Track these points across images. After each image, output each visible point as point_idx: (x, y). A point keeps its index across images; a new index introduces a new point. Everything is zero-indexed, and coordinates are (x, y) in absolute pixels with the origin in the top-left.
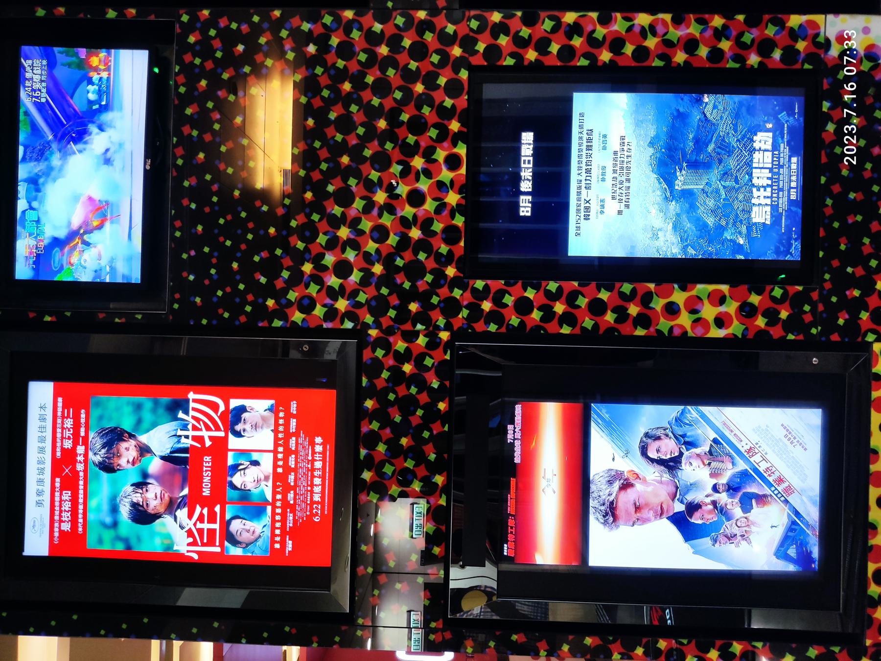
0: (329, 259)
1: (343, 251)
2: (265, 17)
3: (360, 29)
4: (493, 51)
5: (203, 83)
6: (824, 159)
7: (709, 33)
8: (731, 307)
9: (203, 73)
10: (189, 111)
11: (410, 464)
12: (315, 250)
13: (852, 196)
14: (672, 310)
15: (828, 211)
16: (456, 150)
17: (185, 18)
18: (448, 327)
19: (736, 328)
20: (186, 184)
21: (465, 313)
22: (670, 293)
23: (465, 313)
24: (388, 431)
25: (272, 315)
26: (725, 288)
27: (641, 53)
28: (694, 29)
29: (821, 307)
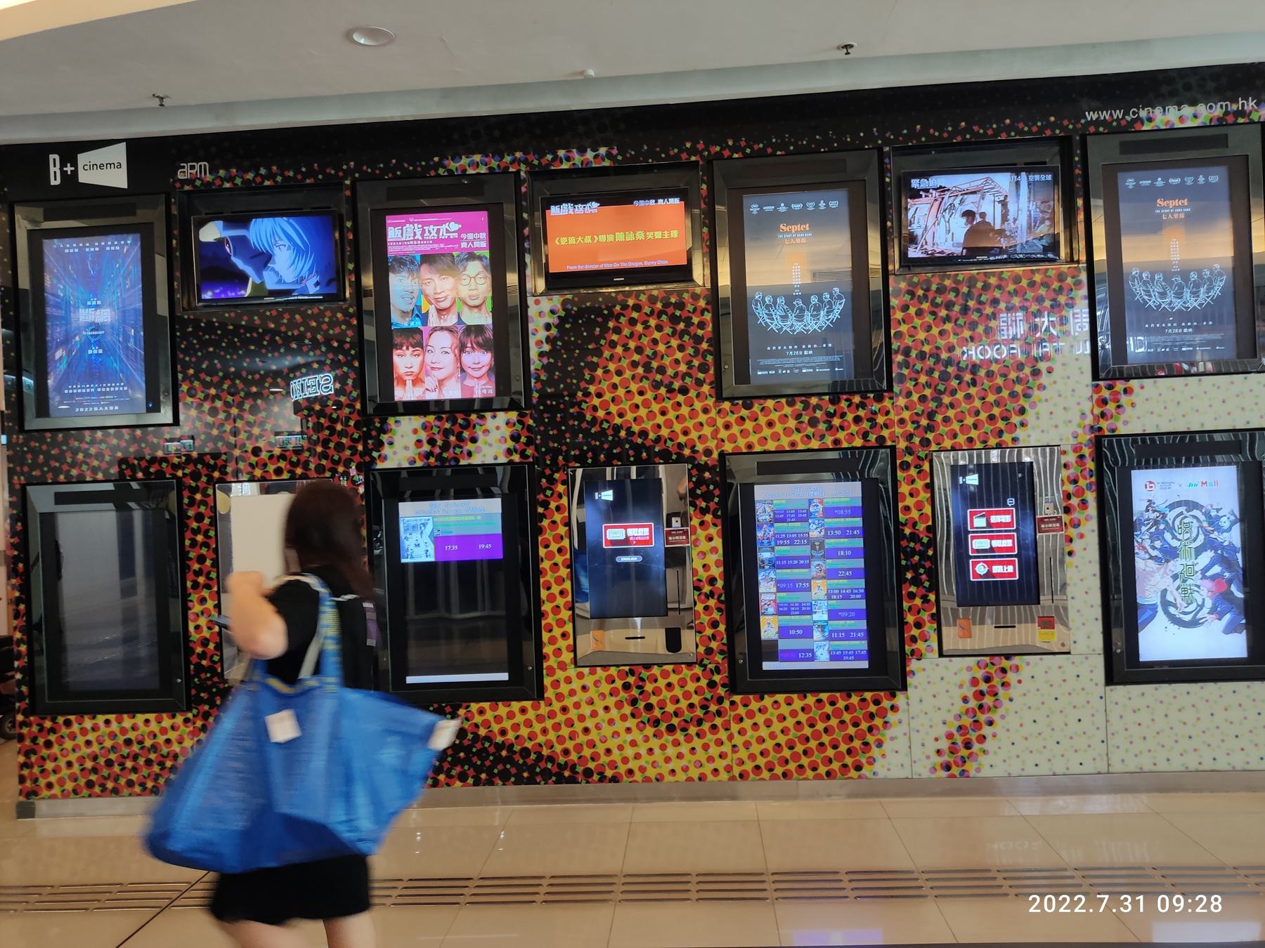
0: (219, 404)
1: (224, 411)
2: (354, 357)
3: (350, 413)
5: (314, 324)
8: (206, 633)
9: (320, 323)
10: (297, 317)
12: (223, 395)
14: (203, 600)
16: (285, 472)
18: (185, 475)
19: (195, 636)
20: (256, 318)
21: (193, 484)
23: (193, 484)
24: (124, 444)
29: (209, 683)
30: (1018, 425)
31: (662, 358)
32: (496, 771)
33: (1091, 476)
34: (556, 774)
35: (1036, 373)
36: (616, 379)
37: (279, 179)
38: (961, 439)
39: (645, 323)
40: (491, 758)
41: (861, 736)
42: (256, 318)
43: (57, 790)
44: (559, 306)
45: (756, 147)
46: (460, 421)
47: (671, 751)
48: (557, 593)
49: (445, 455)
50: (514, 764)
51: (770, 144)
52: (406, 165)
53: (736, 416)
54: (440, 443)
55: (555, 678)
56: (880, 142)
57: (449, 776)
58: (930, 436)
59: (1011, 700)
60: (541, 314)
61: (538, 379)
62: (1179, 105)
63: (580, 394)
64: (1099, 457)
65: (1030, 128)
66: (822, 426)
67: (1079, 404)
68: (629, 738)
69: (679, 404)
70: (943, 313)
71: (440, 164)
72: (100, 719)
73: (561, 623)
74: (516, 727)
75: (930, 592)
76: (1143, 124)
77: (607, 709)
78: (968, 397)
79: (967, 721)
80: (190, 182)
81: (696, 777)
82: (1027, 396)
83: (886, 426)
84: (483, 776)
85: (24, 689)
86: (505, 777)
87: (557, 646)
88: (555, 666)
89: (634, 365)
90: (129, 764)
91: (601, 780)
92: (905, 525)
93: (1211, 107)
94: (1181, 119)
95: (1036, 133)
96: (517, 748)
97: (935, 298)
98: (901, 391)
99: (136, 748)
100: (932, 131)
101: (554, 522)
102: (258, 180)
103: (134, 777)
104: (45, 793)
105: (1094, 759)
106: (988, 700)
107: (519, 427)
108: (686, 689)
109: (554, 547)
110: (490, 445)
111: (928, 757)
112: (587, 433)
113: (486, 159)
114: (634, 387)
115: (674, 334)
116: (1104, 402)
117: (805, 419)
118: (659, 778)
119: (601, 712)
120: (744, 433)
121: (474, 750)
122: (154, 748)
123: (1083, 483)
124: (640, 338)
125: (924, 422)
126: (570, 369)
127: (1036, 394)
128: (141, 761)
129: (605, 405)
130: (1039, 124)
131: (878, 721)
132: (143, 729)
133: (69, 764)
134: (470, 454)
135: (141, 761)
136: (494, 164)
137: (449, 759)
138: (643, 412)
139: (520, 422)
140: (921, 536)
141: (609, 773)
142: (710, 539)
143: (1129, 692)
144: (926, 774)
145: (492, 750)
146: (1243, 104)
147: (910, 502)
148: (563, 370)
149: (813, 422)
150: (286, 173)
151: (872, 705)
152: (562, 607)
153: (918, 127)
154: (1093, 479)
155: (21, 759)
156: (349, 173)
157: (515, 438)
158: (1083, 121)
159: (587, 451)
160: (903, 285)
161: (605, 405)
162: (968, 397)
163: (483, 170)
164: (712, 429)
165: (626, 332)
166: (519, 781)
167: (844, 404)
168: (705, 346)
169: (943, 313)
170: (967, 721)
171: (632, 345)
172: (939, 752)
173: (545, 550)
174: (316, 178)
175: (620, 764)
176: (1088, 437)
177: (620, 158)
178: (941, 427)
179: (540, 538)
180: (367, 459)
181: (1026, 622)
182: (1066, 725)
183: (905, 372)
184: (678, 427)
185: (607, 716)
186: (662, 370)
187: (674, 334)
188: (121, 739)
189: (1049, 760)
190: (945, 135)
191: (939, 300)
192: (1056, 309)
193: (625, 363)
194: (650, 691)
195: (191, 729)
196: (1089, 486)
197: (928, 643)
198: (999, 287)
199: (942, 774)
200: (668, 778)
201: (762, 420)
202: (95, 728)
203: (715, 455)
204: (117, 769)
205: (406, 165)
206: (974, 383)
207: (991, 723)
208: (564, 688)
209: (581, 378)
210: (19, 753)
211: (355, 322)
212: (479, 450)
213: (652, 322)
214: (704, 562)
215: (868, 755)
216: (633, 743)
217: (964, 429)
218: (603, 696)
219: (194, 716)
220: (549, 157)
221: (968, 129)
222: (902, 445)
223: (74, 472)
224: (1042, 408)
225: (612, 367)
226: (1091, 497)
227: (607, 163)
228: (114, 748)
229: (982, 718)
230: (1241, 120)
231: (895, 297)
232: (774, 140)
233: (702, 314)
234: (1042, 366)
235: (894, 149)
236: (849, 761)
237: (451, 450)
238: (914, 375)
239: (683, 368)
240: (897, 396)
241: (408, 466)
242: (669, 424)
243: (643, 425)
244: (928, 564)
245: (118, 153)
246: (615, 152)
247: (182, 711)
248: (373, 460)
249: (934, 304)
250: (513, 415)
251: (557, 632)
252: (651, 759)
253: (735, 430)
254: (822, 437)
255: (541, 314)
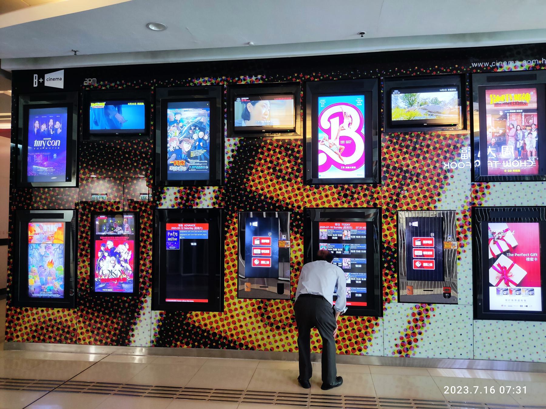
2: (151, 161)
4: (143, 217)
5: (136, 147)
6: (118, 297)
7: (147, 269)
8: (84, 275)
10: (129, 143)
11: (49, 200)
13: (110, 304)
14: (84, 261)
15: (106, 298)
17: (151, 141)
19: (80, 277)
22: (88, 261)
25: (82, 165)
26: (89, 274)
27: (143, 253)
28: (148, 266)
29: (84, 297)
30: (437, 200)
31: (281, 166)
32: (202, 342)
33: (470, 225)
34: (227, 345)
35: (446, 178)
36: (261, 174)
37: (125, 86)
38: (411, 206)
39: (274, 150)
40: (200, 336)
41: (361, 336)
42: (112, 143)
43: (20, 339)
44: (238, 142)
45: (325, 76)
46: (194, 190)
47: (278, 338)
48: (231, 266)
49: (187, 204)
50: (210, 339)
51: (331, 75)
52: (177, 81)
53: (312, 192)
54: (185, 199)
55: (229, 302)
56: (379, 75)
57: (181, 343)
58: (397, 204)
59: (430, 324)
60: (230, 145)
61: (228, 173)
62: (514, 61)
63: (245, 180)
64: (473, 217)
65: (446, 70)
66: (349, 198)
67: (465, 192)
68: (259, 331)
69: (287, 186)
70: (405, 150)
71: (191, 81)
72: (40, 309)
73: (232, 279)
74: (211, 323)
75: (395, 273)
76: (498, 69)
77: (250, 317)
78: (415, 187)
79: (409, 332)
80: (89, 86)
81: (288, 350)
82: (441, 188)
83: (378, 199)
84: (196, 344)
85: (10, 295)
86: (205, 345)
87: (230, 289)
88: (229, 297)
89: (269, 168)
90: (50, 329)
91: (246, 349)
92: (384, 243)
93: (529, 62)
94: (515, 67)
95: (449, 72)
96: (211, 332)
97: (401, 143)
98: (385, 183)
99: (53, 322)
100: (402, 70)
101: (231, 235)
102: (116, 86)
103: (52, 335)
104: (16, 339)
105: (467, 353)
106: (420, 323)
107: (218, 193)
108: (285, 310)
109: (231, 245)
110: (206, 200)
111: (391, 347)
112: (247, 196)
113: (210, 79)
114: (268, 178)
115: (286, 155)
116: (476, 192)
117: (342, 194)
118: (272, 349)
119: (248, 318)
120: (315, 199)
121: (193, 332)
122: (61, 323)
123: (466, 227)
124: (272, 157)
125: (395, 198)
126: (241, 169)
127: (446, 187)
128: (55, 328)
129: (255, 185)
130: (451, 68)
131: (370, 330)
132: (57, 315)
133: (26, 328)
134: (197, 204)
135: (55, 328)
136: (213, 81)
137: (182, 335)
138: (272, 189)
139: (219, 191)
140: (392, 248)
141: (250, 346)
142: (298, 245)
143: (484, 323)
144: (390, 355)
145: (200, 332)
146: (544, 61)
147: (387, 232)
148: (238, 169)
149: (346, 196)
150: (128, 84)
151: (347, 321)
152: (233, 272)
153: (396, 69)
154: (471, 226)
155: (7, 324)
156: (153, 84)
157: (217, 197)
158: (470, 67)
159: (247, 205)
160: (387, 137)
161: (255, 185)
162: (415, 187)
163: (209, 84)
164: (301, 197)
165: (266, 154)
166: (212, 347)
167: (359, 188)
168: (299, 161)
169: (405, 150)
170: (409, 332)
171: (268, 159)
172: (396, 345)
173: (227, 247)
174: (140, 86)
175: (255, 342)
176: (469, 207)
177: (266, 80)
178: (403, 200)
179: (225, 241)
180: (154, 204)
181: (438, 287)
182: (455, 336)
183: (387, 175)
184: (286, 196)
185: (250, 321)
186: (280, 171)
187: (286, 155)
188: (47, 318)
189: (447, 352)
190: (408, 72)
191: (403, 144)
192: (456, 150)
193: (265, 167)
194: (270, 311)
195: (76, 316)
196: (469, 229)
197: (393, 296)
198: (430, 139)
199: (397, 355)
200: (276, 350)
201: (323, 194)
202: (37, 313)
203: (302, 208)
204: (45, 331)
205: (177, 81)
206: (417, 181)
207: (420, 333)
208: (233, 307)
209: (246, 173)
210: (6, 322)
211: (152, 146)
212: (201, 202)
213: (277, 150)
214: (296, 255)
215: (364, 345)
216: (261, 333)
217: (413, 201)
218: (249, 312)
219: (77, 310)
220: (237, 79)
221: (419, 70)
222: (385, 207)
223: (35, 205)
224: (448, 193)
225: (259, 169)
226: (469, 234)
227: (261, 82)
228: (44, 322)
229: (416, 331)
230: (543, 68)
231: (384, 142)
232: (333, 73)
233: (299, 147)
234: (449, 175)
235: (385, 78)
236: (356, 347)
237: (190, 202)
238: (391, 177)
239: (290, 170)
240: (383, 186)
241: (171, 208)
242: (282, 194)
243: (272, 194)
244: (394, 261)
245: (61, 74)
246: (264, 77)
247: (73, 308)
248: (157, 205)
249: (401, 146)
250: (216, 188)
251: (231, 282)
252: (269, 340)
253: (311, 198)
254: (349, 202)
255: (230, 145)
